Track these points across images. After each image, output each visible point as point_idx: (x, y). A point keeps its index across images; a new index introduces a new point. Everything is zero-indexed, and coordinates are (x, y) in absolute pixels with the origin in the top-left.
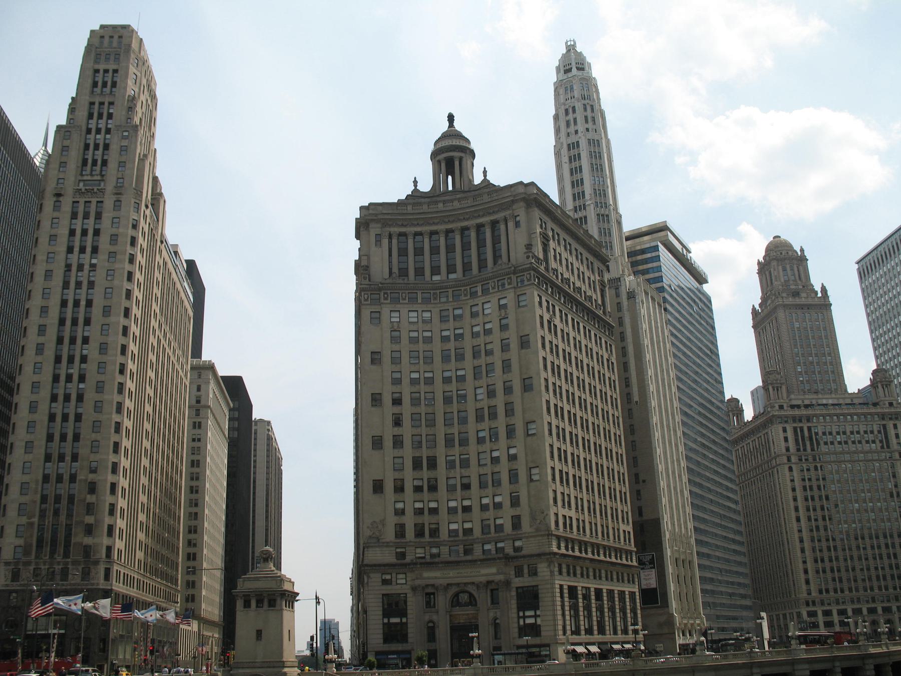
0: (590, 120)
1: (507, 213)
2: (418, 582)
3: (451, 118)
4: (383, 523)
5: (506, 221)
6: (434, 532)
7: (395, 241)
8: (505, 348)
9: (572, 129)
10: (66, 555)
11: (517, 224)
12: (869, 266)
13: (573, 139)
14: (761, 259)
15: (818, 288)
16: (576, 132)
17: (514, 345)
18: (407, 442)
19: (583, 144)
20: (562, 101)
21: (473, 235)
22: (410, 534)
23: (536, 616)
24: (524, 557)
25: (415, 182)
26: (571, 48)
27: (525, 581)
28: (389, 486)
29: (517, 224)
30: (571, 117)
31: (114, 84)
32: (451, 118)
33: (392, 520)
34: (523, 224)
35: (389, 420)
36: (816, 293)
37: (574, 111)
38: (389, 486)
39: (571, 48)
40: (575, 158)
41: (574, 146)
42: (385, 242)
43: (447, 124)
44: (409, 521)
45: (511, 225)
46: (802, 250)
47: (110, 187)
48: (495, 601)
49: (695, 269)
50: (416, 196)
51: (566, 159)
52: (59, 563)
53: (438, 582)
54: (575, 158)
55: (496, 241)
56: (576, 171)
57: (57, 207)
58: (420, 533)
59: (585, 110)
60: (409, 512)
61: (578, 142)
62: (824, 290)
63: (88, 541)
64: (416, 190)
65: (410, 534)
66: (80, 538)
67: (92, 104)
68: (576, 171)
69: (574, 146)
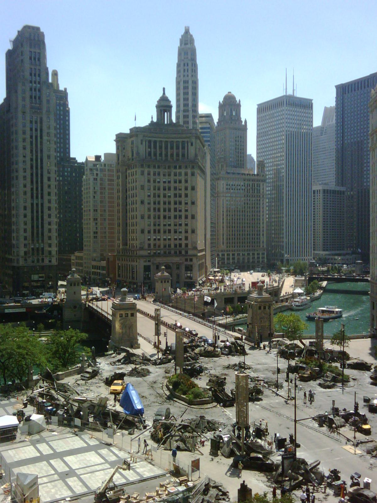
0: (193, 71)
1: (188, 140)
2: (155, 262)
3: (164, 89)
4: (144, 242)
5: (188, 142)
6: (159, 246)
7: (147, 143)
8: (186, 189)
9: (186, 73)
10: (43, 254)
11: (192, 145)
12: (264, 109)
13: (186, 79)
14: (221, 102)
15: (243, 120)
16: (188, 76)
17: (189, 188)
18: (152, 217)
19: (190, 82)
20: (183, 58)
21: (175, 144)
22: (152, 247)
23: (191, 273)
24: (189, 256)
25: (152, 118)
26: (187, 32)
27: (189, 263)
28: (146, 232)
29: (192, 145)
30: (186, 68)
31: (39, 60)
32: (164, 89)
33: (147, 242)
34: (194, 144)
35: (146, 210)
36: (242, 122)
37: (188, 65)
38: (146, 232)
39: (187, 32)
40: (186, 88)
41: (186, 82)
42: (144, 143)
43: (162, 92)
44: (152, 242)
45: (190, 144)
46: (240, 101)
47: (45, 109)
48: (178, 268)
49: (204, 115)
50: (152, 123)
51: (182, 87)
52: (40, 257)
53: (161, 262)
54: (186, 88)
55: (183, 148)
56: (186, 94)
57: (24, 118)
58: (155, 245)
59: (192, 66)
60: (152, 240)
61: (188, 81)
62: (246, 122)
63: (50, 249)
64: (152, 121)
65: (152, 247)
66: (47, 248)
67: (31, 69)
68: (186, 94)
69: (186, 82)
